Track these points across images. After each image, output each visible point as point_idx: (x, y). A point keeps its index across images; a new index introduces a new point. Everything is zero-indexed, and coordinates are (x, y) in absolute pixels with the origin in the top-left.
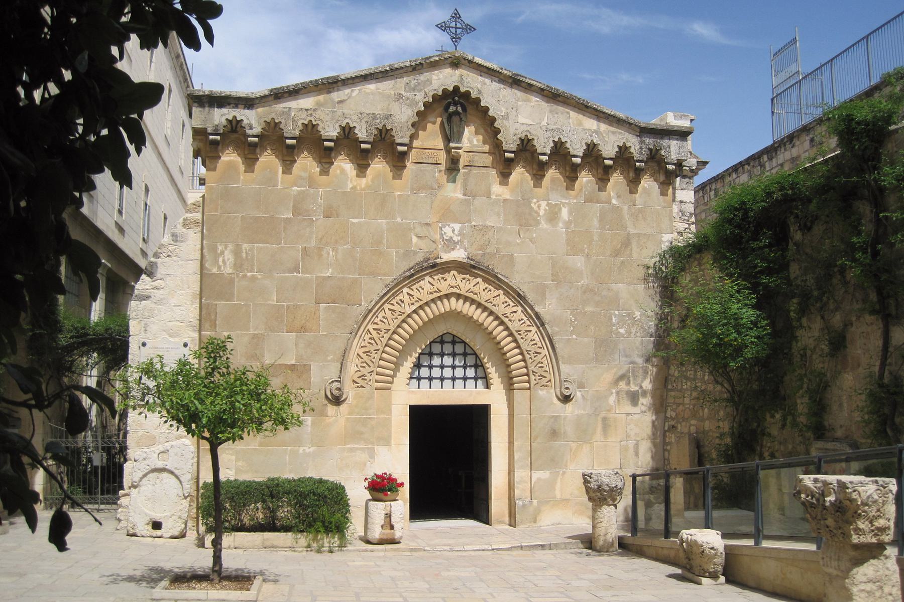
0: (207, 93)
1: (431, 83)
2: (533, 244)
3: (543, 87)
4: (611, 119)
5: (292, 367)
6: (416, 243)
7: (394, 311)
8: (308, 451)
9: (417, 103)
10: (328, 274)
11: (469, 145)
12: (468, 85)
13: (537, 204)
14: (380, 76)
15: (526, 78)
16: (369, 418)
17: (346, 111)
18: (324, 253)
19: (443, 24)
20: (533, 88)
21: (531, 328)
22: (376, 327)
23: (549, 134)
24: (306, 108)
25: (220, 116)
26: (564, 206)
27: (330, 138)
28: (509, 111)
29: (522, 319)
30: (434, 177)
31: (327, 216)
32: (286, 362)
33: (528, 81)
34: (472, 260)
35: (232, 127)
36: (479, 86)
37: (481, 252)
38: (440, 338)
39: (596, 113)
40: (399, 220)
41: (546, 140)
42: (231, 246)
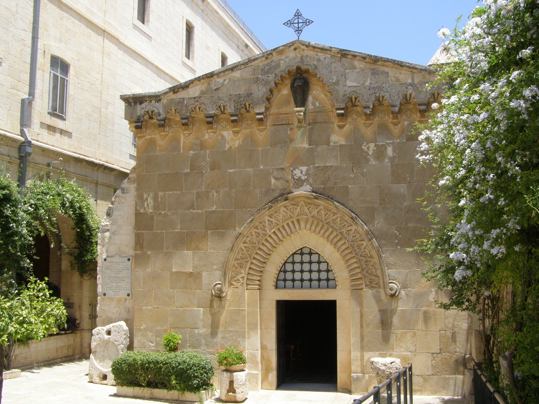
0: (131, 96)
1: (280, 66)
2: (364, 177)
3: (364, 56)
4: (423, 73)
5: (191, 274)
6: (274, 184)
7: (259, 234)
8: (201, 331)
9: (270, 82)
10: (213, 209)
11: (312, 107)
12: (307, 63)
13: (368, 145)
14: (243, 67)
15: (350, 51)
16: (241, 310)
17: (220, 95)
18: (211, 194)
19: (289, 22)
20: (357, 58)
21: (363, 242)
22: (246, 245)
23: (372, 91)
24: (194, 97)
25: (140, 110)
26: (389, 146)
27: (209, 115)
28: (339, 79)
29: (355, 236)
30: (287, 133)
31: (213, 168)
32: (186, 271)
33: (352, 53)
34: (316, 193)
35: (150, 116)
36: (315, 63)
37: (322, 186)
38: (300, 250)
39: (411, 70)
40: (262, 167)
41: (369, 96)
42: (151, 195)
